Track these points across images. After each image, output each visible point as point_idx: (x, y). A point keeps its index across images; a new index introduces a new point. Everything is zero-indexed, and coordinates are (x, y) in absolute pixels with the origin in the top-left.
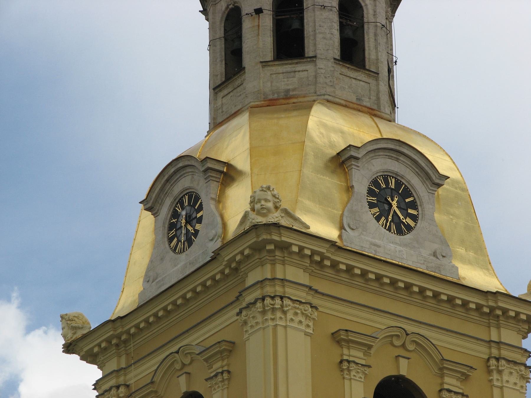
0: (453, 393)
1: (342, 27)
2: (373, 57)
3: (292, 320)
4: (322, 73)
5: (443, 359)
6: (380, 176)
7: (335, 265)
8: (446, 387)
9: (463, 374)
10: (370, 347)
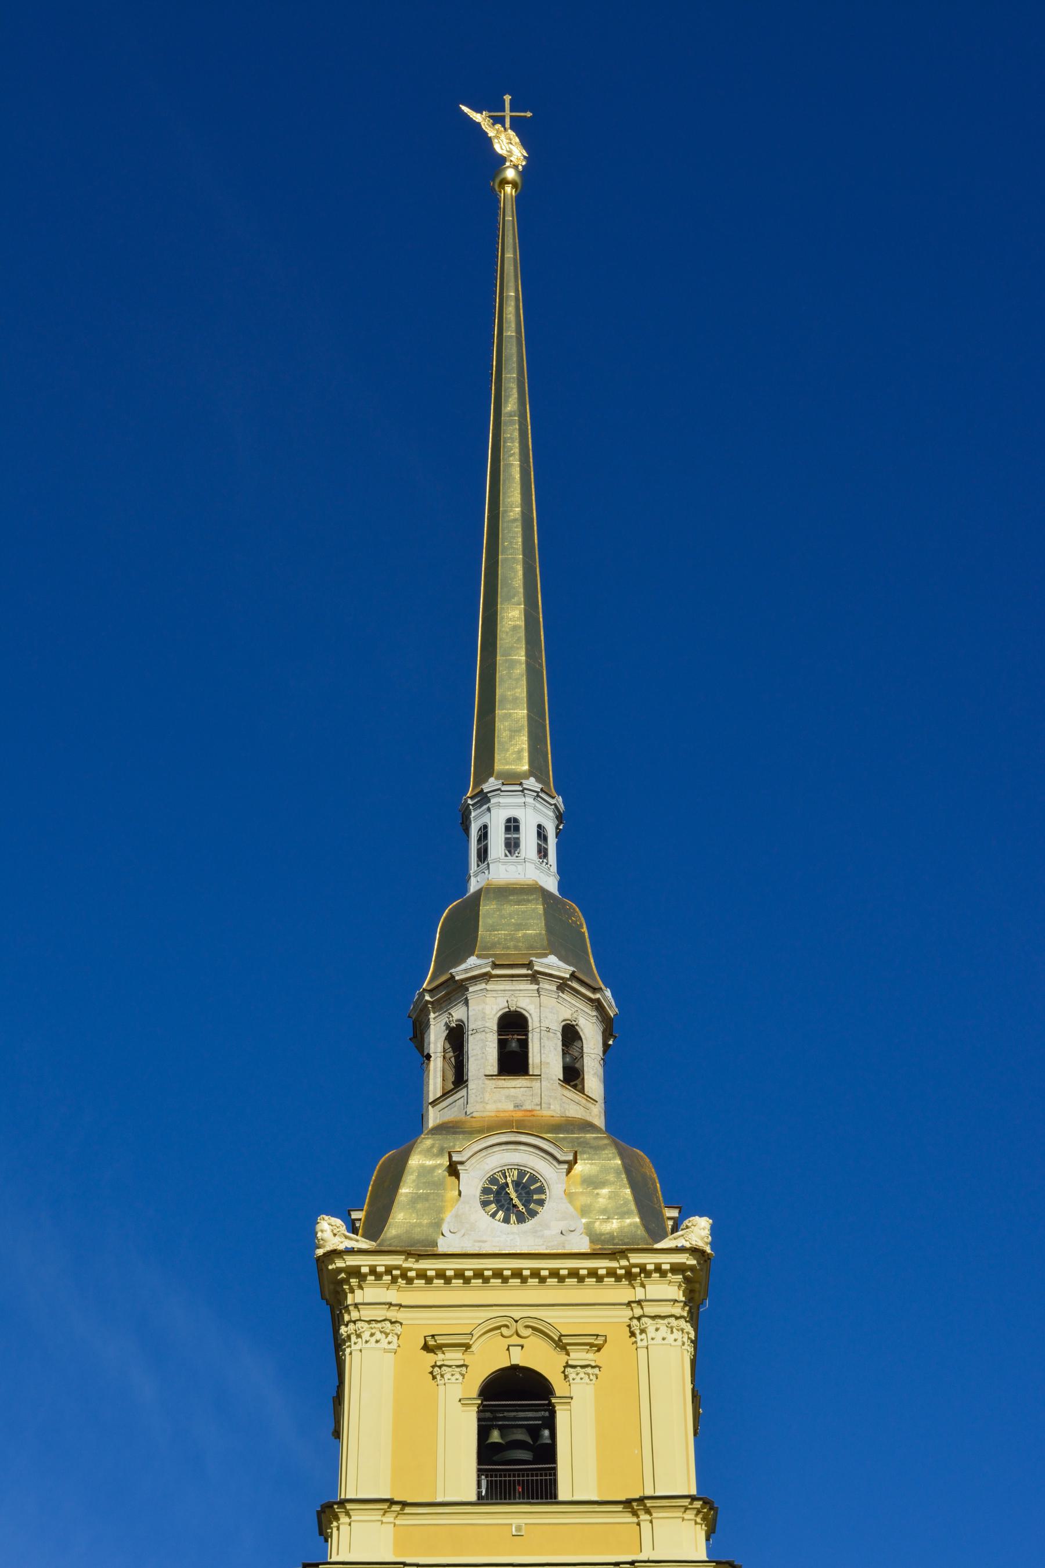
0: (590, 1368)
1: (502, 1044)
2: (537, 1060)
3: (367, 1342)
4: (473, 1093)
5: (562, 1335)
6: (498, 1172)
7: (422, 1275)
8: (570, 1363)
9: (591, 1345)
10: (467, 1347)
